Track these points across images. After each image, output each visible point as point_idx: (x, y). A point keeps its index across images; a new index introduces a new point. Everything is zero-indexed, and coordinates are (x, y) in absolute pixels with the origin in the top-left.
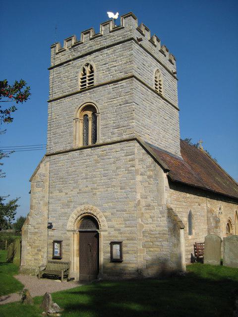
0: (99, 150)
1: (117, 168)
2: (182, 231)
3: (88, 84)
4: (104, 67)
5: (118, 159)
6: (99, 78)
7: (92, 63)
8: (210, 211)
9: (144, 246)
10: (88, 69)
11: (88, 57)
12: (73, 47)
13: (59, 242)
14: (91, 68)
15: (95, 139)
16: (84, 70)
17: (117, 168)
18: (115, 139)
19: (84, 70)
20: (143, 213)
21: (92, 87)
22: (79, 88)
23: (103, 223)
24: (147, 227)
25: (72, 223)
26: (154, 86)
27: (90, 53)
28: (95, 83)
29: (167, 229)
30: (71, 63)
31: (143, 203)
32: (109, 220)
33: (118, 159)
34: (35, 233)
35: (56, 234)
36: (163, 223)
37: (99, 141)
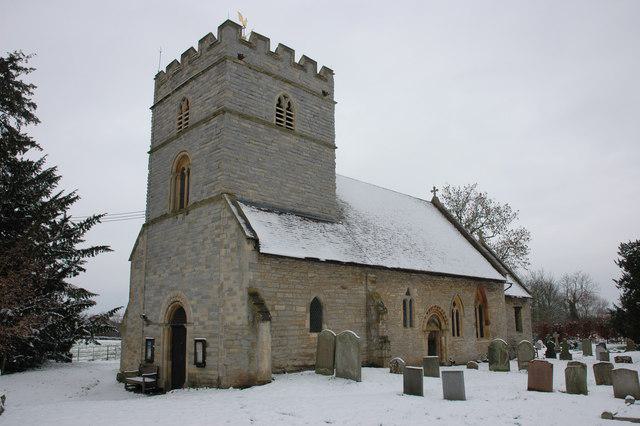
1: (204, 240)
2: (265, 327)
4: (199, 101)
5: (206, 227)
6: (196, 113)
8: (370, 297)
10: (184, 107)
11: (186, 89)
17: (204, 240)
23: (191, 315)
25: (161, 316)
26: (275, 118)
29: (246, 322)
32: (195, 311)
33: (206, 227)
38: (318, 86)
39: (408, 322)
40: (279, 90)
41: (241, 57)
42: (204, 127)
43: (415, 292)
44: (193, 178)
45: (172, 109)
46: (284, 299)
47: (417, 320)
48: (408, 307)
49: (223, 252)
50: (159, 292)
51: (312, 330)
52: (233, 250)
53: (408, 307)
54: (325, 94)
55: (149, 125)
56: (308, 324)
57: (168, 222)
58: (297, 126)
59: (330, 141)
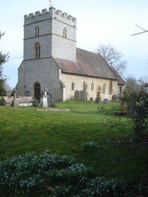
0: (41, 60)
1: (46, 67)
3: (37, 36)
5: (47, 64)
6: (42, 32)
7: (39, 26)
8: (84, 83)
9: (53, 93)
10: (37, 29)
12: (32, 18)
13: (28, 92)
14: (38, 28)
15: (39, 56)
16: (36, 29)
17: (46, 67)
18: (46, 57)
19: (36, 29)
20: (53, 83)
21: (39, 36)
22: (34, 36)
23: (42, 85)
24: (54, 87)
25: (32, 86)
27: (38, 22)
28: (40, 35)
29: (60, 88)
30: (31, 25)
31: (53, 79)
33: (47, 64)
34: (20, 89)
35: (27, 89)
36: (59, 85)
37: (41, 57)
38: (72, 24)
39: (92, 89)
40: (64, 26)
41: (55, 18)
42: (45, 37)
43: (94, 82)
44: (41, 50)
45: (32, 28)
46: (66, 82)
47: (94, 89)
48: (92, 85)
49: (53, 71)
50: (30, 79)
51: (72, 90)
52: (55, 70)
53: (92, 85)
54: (74, 26)
55: (23, 31)
56: (71, 89)
57: (33, 61)
58: (68, 37)
59: (75, 40)
